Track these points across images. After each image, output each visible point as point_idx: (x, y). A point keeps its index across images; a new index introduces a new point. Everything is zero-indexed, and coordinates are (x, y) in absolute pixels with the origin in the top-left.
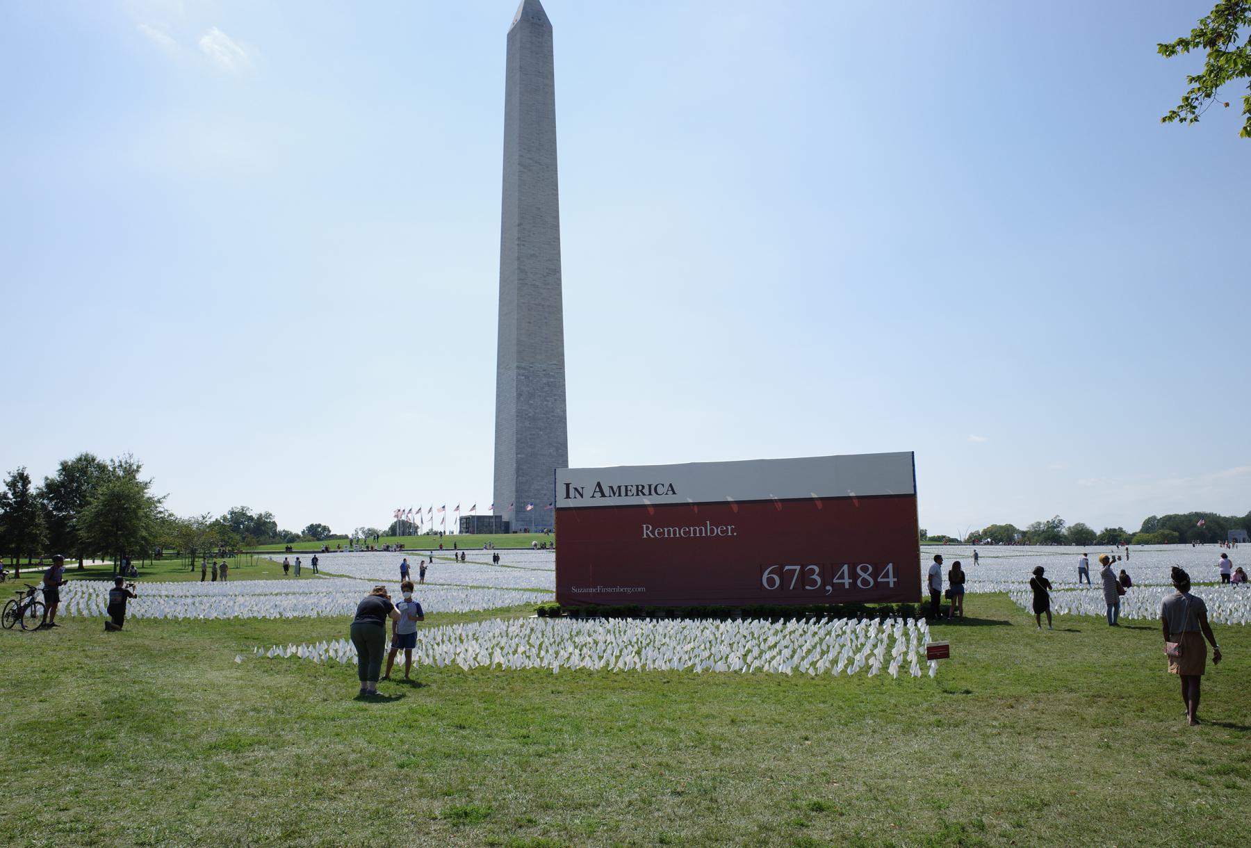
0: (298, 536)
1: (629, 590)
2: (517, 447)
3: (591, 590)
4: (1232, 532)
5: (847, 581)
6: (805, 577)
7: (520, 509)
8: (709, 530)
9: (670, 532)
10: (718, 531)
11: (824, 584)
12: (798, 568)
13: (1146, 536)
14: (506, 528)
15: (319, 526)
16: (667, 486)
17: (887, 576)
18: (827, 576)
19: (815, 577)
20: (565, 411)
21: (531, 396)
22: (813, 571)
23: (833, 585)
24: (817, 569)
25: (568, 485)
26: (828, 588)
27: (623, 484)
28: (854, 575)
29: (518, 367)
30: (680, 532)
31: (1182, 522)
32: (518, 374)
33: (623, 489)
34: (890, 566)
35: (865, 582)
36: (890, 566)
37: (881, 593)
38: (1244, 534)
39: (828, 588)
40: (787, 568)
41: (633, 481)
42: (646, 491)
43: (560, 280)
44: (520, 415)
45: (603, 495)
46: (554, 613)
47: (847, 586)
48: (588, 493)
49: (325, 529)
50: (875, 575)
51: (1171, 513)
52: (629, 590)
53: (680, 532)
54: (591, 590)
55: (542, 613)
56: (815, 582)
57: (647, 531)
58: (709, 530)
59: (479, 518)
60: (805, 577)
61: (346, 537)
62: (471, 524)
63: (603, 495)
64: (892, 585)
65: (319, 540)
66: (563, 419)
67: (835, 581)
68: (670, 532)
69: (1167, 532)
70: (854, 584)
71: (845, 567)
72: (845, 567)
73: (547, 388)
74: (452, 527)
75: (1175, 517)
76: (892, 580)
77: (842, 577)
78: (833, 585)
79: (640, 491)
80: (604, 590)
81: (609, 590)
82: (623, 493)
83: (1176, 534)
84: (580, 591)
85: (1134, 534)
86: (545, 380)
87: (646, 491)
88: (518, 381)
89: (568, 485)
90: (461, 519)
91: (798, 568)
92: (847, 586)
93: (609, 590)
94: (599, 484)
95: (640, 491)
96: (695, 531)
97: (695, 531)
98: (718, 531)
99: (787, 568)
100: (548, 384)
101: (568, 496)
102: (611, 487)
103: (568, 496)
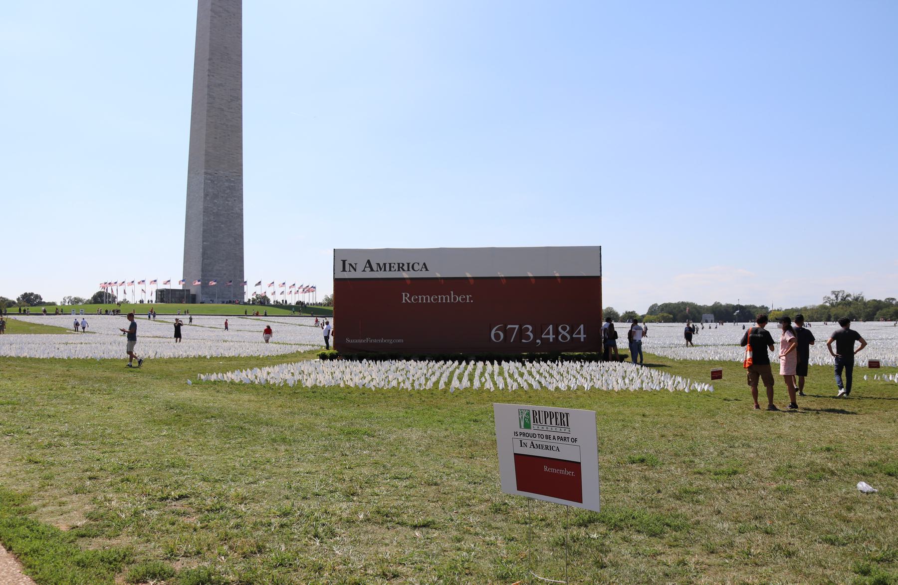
0: (14, 302)
1: (391, 341)
2: (203, 237)
4: (704, 316)
5: (551, 337)
6: (522, 333)
7: (205, 285)
8: (452, 298)
9: (422, 299)
10: (459, 299)
11: (535, 339)
12: (517, 327)
13: (652, 317)
14: (193, 299)
15: (32, 294)
16: (421, 264)
17: (579, 333)
18: (538, 332)
19: (529, 333)
20: (242, 210)
21: (216, 196)
22: (527, 329)
23: (542, 339)
24: (530, 328)
25: (344, 262)
26: (538, 341)
27: (388, 262)
28: (556, 333)
29: (206, 173)
30: (431, 299)
31: (675, 308)
32: (206, 179)
33: (388, 268)
34: (582, 327)
35: (564, 337)
36: (582, 327)
37: (575, 345)
38: (712, 317)
39: (538, 341)
40: (509, 326)
41: (395, 260)
42: (405, 268)
44: (206, 211)
45: (372, 270)
46: (332, 357)
47: (551, 340)
48: (360, 268)
49: (37, 297)
50: (571, 333)
51: (667, 302)
52: (391, 341)
53: (431, 299)
55: (323, 357)
57: (405, 298)
58: (452, 298)
60: (522, 333)
61: (54, 304)
62: (164, 296)
63: (372, 270)
65: (32, 305)
66: (240, 216)
67: (543, 336)
68: (422, 299)
69: (665, 315)
70: (556, 339)
71: (551, 327)
72: (551, 327)
73: (228, 191)
74: (150, 296)
75: (670, 304)
76: (582, 336)
77: (548, 333)
78: (542, 339)
79: (400, 267)
80: (371, 341)
81: (375, 341)
82: (388, 268)
83: (671, 316)
84: (353, 341)
85: (643, 316)
86: (226, 184)
87: (405, 268)
89: (344, 262)
90: (157, 291)
91: (517, 327)
92: (551, 340)
93: (375, 341)
94: (369, 262)
95: (400, 267)
96: (442, 299)
97: (442, 299)
98: (459, 299)
99: (509, 326)
100: (229, 187)
101: (344, 270)
102: (378, 264)
103: (344, 270)
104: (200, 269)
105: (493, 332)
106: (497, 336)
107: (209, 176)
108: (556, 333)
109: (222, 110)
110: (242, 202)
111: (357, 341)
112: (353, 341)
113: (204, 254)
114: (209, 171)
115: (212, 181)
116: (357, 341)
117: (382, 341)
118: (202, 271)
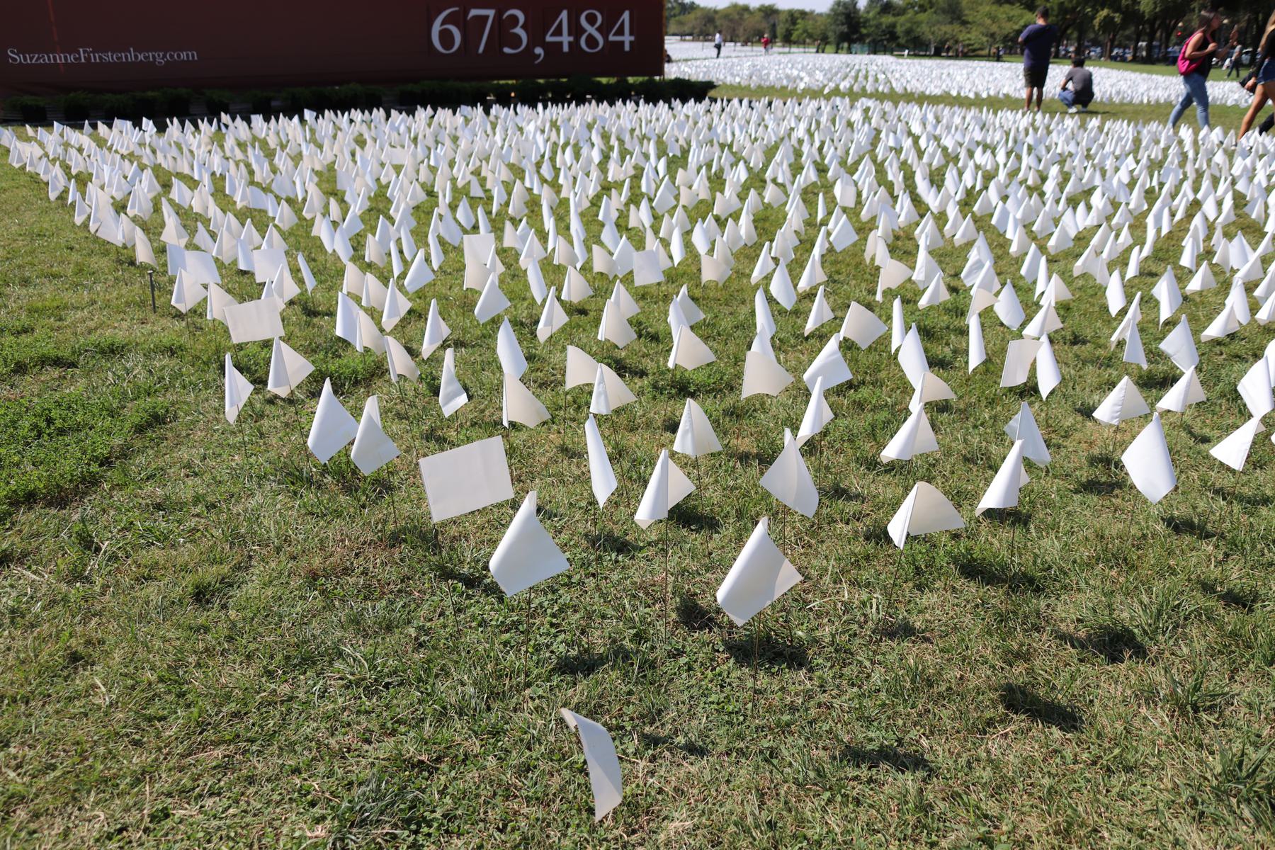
1: (159, 58)
3: (60, 58)
5: (566, 39)
6: (503, 29)
18: (537, 29)
19: (519, 31)
22: (514, 19)
23: (546, 46)
28: (576, 30)
37: (613, 59)
47: (566, 48)
50: (604, 30)
52: (159, 58)
54: (60, 58)
56: (518, 38)
64: (627, 48)
67: (549, 39)
70: (574, 45)
71: (564, 15)
72: (564, 15)
76: (627, 39)
77: (558, 32)
78: (546, 46)
80: (96, 58)
81: (110, 57)
84: (33, 59)
92: (566, 48)
93: (110, 57)
105: (436, 27)
106: (446, 37)
108: (576, 30)
111: (46, 59)
112: (33, 59)
116: (46, 59)
117: (131, 56)
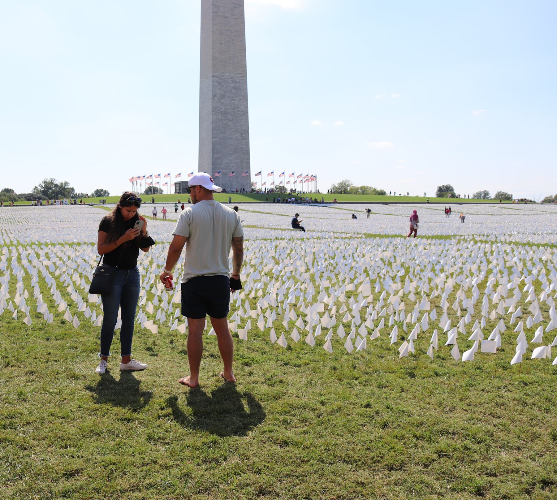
2: (213, 134)
21: (223, 96)
29: (213, 76)
32: (213, 81)
43: (243, 11)
44: (214, 110)
59: (183, 182)
66: (245, 113)
73: (234, 91)
86: (232, 85)
88: (213, 86)
100: (235, 88)
104: (211, 163)
107: (216, 79)
109: (226, 17)
110: (247, 100)
113: (214, 149)
114: (217, 74)
115: (219, 83)
118: (213, 164)
